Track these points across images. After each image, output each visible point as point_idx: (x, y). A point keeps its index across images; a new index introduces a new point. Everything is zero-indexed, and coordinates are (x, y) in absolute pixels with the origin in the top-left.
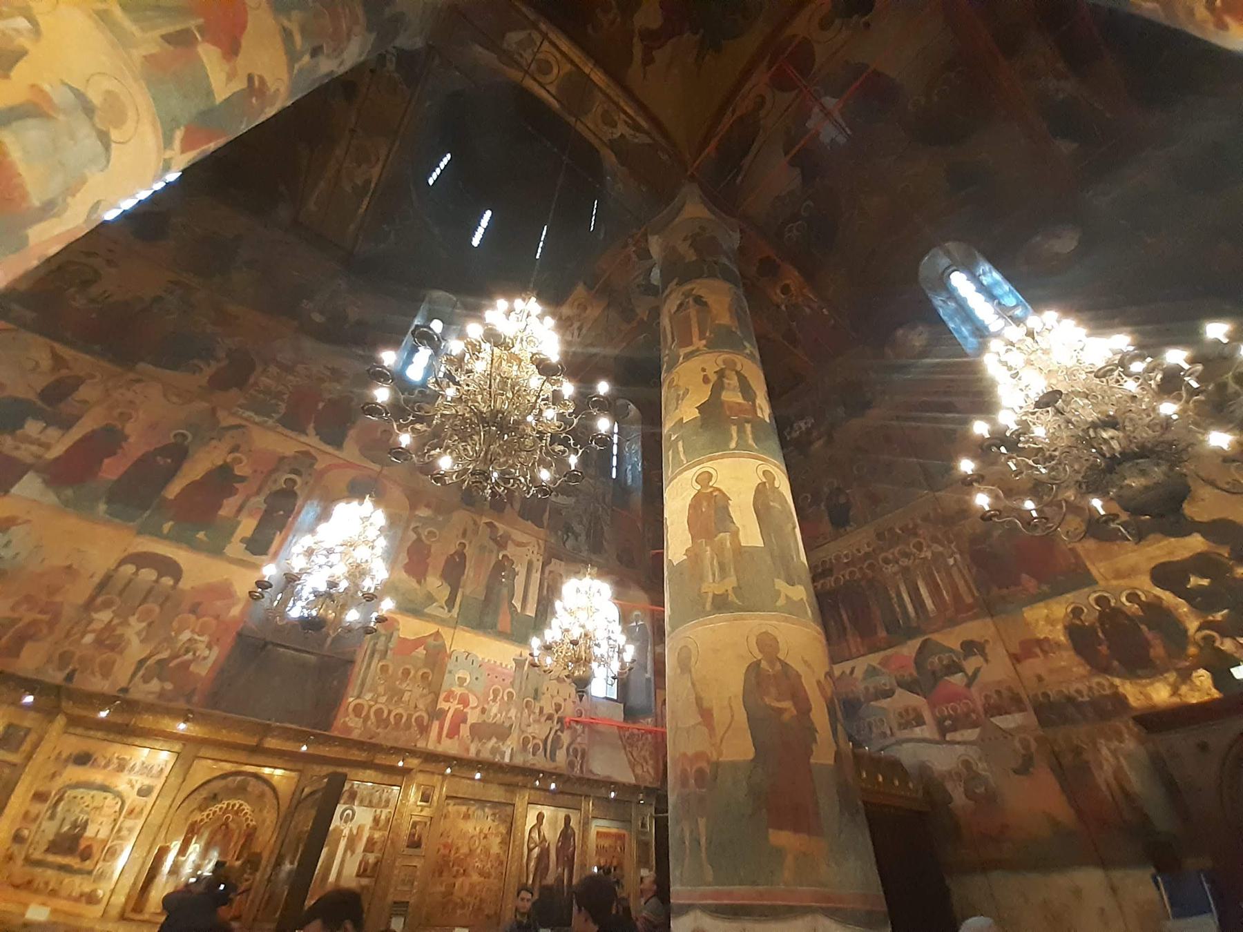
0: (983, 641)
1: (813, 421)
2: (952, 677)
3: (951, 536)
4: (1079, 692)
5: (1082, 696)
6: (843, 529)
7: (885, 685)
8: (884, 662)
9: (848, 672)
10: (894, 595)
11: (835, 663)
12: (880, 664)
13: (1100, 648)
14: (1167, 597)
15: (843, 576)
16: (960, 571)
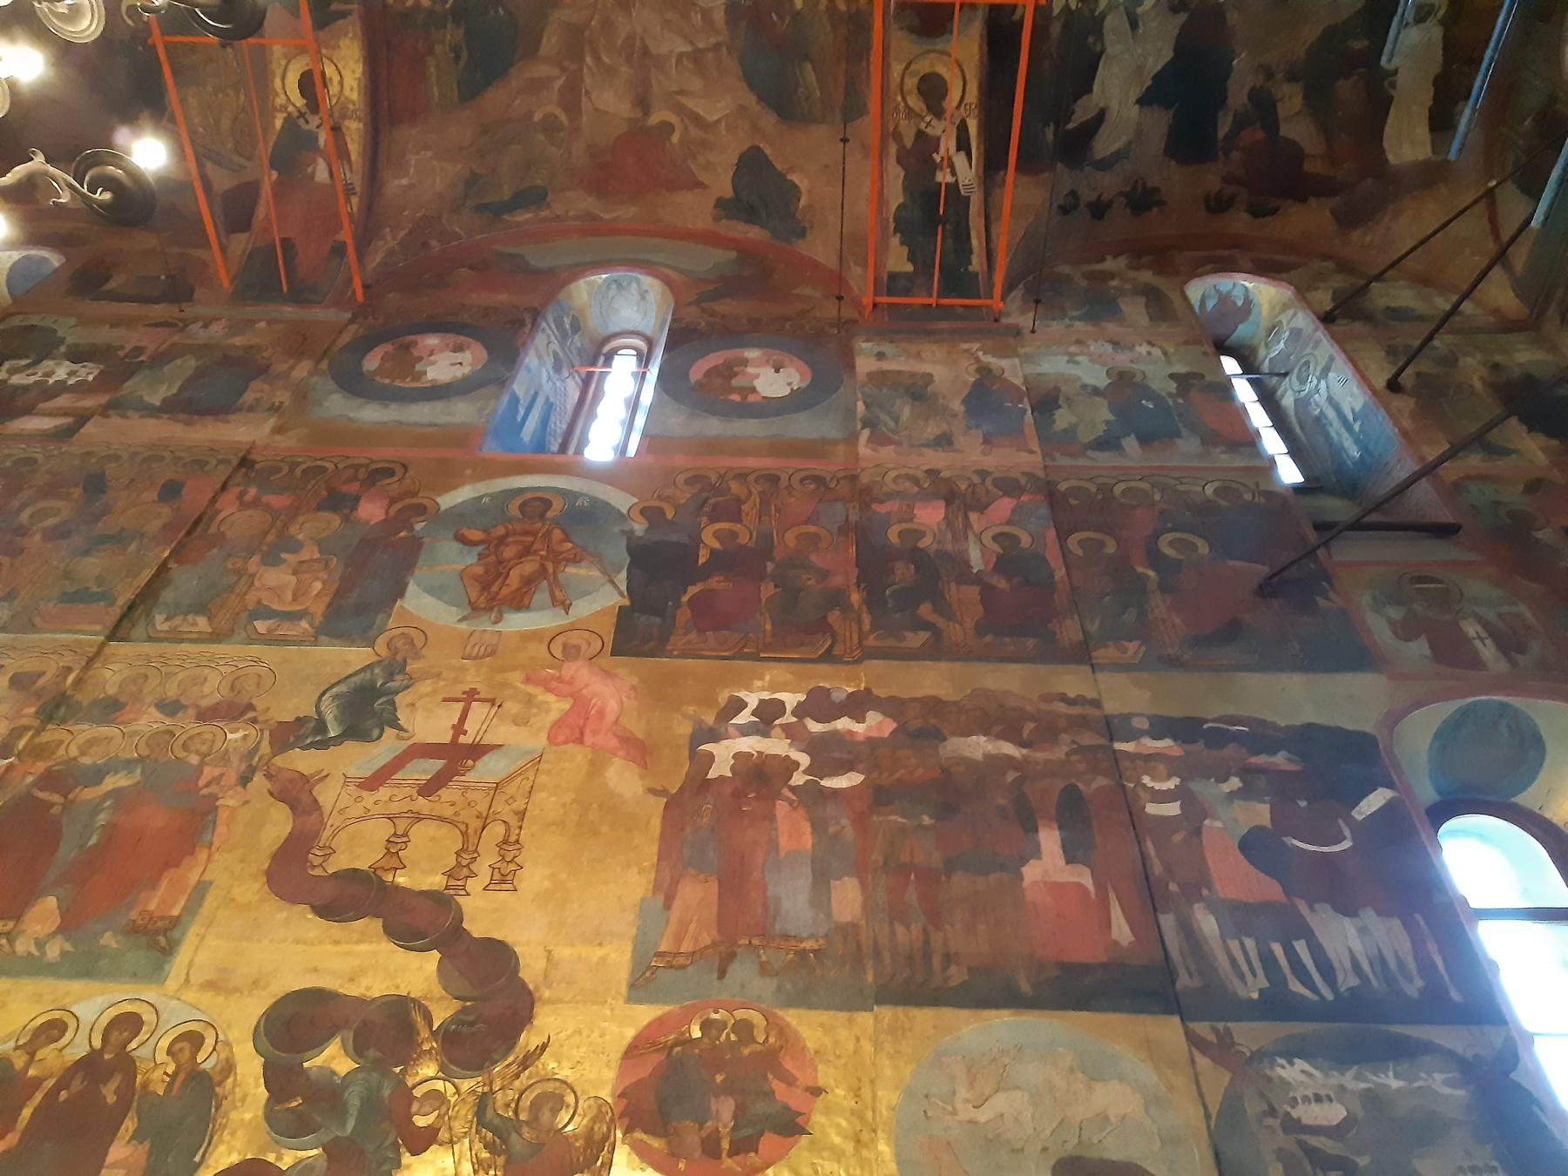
1: (90, 378)
3: (22, 744)
14: (250, 1068)
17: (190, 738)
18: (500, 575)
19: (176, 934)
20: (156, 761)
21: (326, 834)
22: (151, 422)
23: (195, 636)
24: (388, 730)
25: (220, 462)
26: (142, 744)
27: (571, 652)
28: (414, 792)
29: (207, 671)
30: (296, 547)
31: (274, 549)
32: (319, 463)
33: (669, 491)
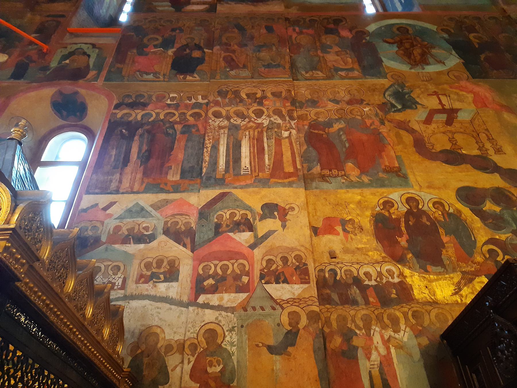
0: (287, 207)
2: (238, 234)
3: (295, 115)
4: (367, 274)
5: (370, 280)
6: (182, 77)
7: (146, 229)
8: (156, 207)
9: (101, 206)
10: (209, 145)
11: (88, 193)
12: (152, 206)
13: (399, 239)
14: (466, 212)
15: (158, 114)
16: (291, 144)
17: (351, 110)
18: (411, 53)
19: (403, 171)
20: (346, 119)
21: (426, 139)
22: (240, 5)
23: (322, 78)
24: (418, 106)
25: (279, 19)
26: (336, 114)
27: (458, 78)
28: (444, 124)
29: (337, 89)
30: (331, 47)
31: (325, 49)
32: (312, 18)
33: (445, 23)
